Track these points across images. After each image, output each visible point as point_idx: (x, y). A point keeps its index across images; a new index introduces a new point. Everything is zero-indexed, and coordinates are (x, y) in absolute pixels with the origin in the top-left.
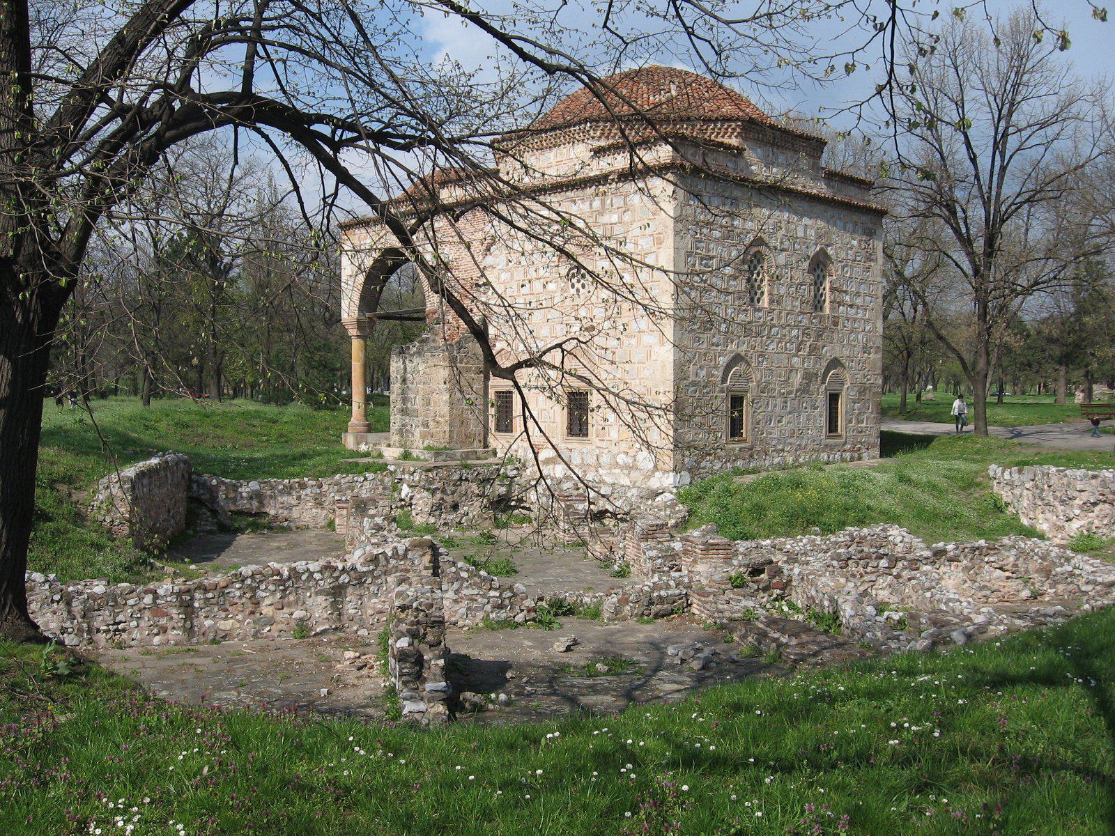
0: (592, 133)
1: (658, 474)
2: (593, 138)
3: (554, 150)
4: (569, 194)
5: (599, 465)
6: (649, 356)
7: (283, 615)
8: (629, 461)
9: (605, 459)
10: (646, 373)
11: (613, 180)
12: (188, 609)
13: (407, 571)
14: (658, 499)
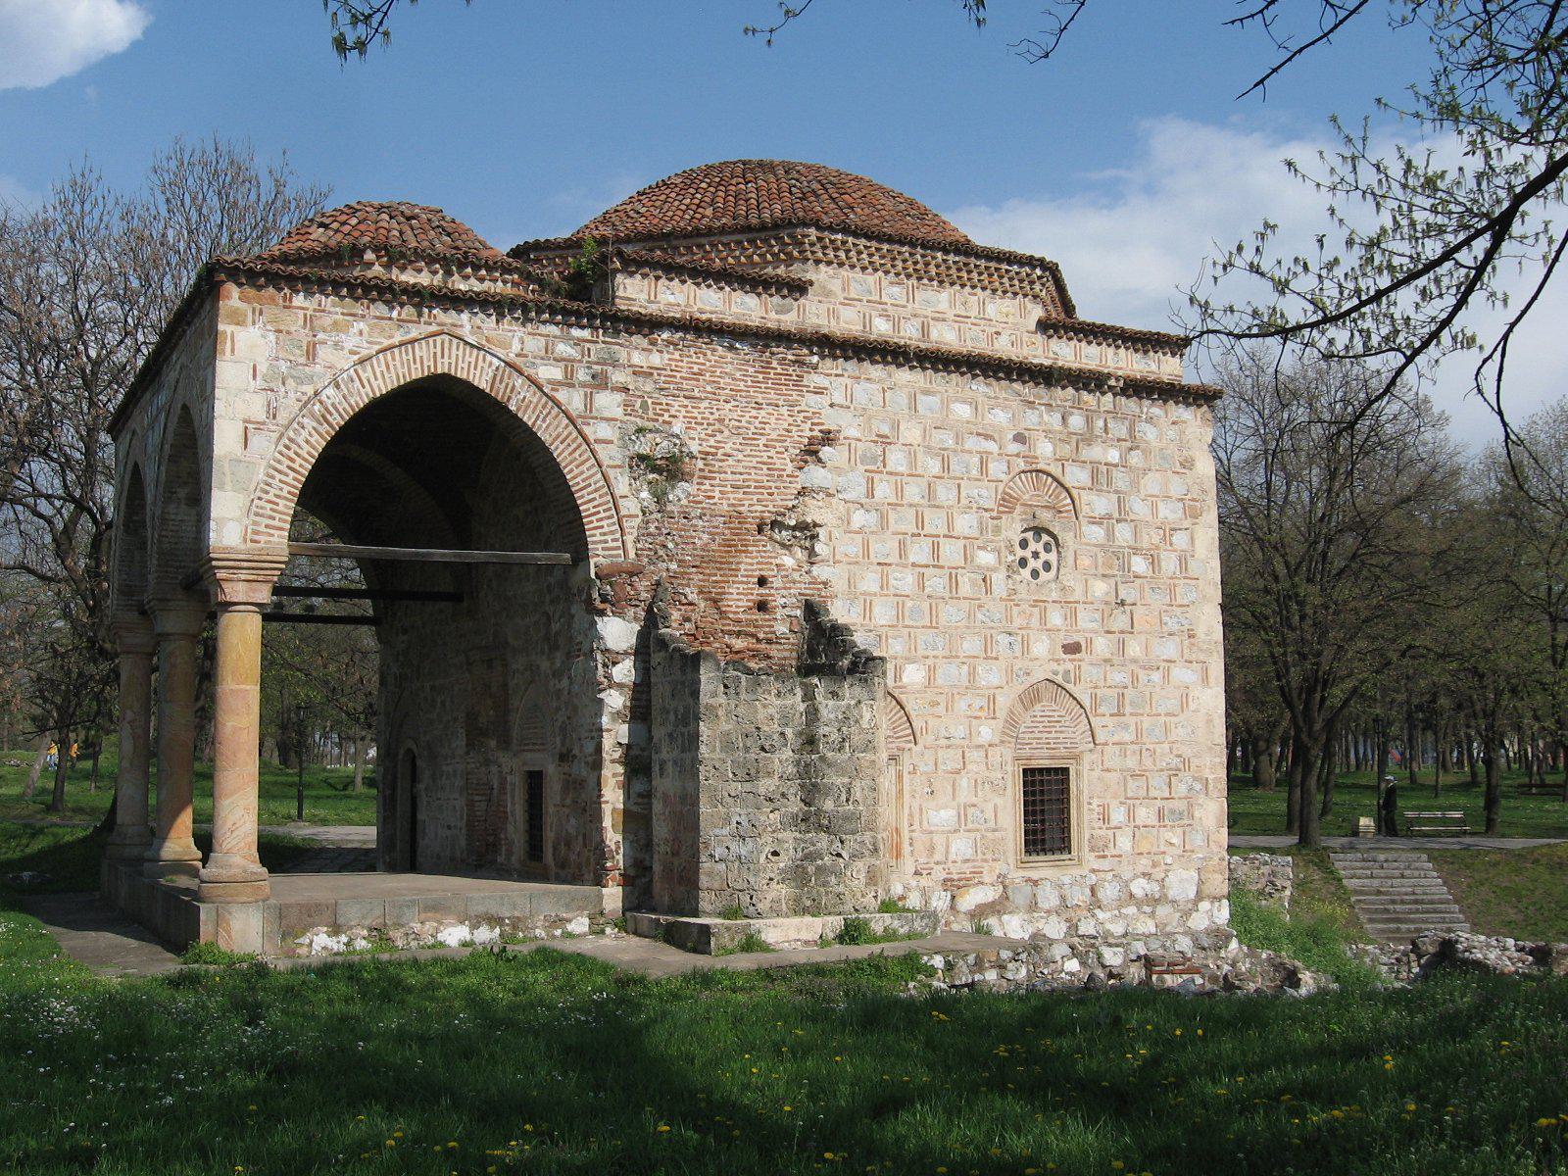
0: (1037, 287)
1: (1204, 905)
2: (1035, 297)
4: (1017, 386)
5: (1095, 903)
6: (1184, 701)
9: (1109, 892)
11: (1111, 388)
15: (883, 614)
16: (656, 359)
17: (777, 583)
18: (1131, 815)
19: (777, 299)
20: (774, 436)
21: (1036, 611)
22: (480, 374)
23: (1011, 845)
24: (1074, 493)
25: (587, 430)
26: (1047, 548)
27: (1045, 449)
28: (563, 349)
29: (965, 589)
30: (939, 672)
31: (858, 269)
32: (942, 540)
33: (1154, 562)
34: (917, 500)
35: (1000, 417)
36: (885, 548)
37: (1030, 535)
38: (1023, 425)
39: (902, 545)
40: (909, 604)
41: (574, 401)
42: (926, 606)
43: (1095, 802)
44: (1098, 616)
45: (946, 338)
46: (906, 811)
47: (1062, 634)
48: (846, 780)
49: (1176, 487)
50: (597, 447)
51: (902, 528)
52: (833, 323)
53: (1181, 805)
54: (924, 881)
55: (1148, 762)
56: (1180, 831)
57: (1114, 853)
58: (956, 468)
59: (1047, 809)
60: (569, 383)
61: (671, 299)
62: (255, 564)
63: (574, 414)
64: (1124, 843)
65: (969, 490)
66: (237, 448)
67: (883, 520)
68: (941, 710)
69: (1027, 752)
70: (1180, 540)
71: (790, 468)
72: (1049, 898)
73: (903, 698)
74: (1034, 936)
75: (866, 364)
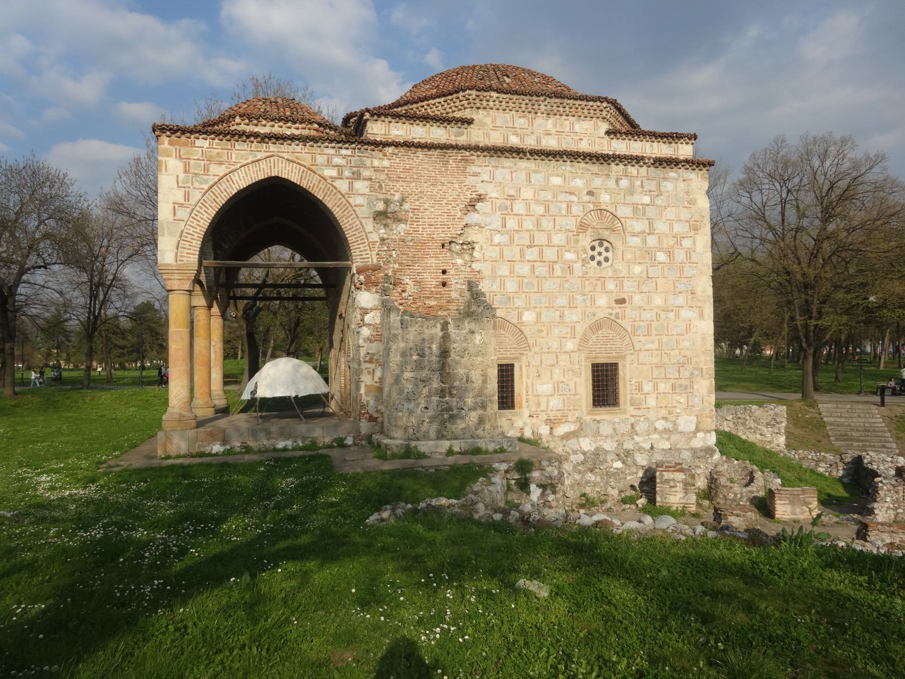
0: (604, 113)
1: (700, 435)
6: (688, 329)
8: (670, 425)
9: (641, 427)
10: (686, 344)
15: (511, 286)
16: (386, 163)
17: (452, 272)
18: (655, 387)
19: (455, 129)
20: (451, 198)
21: (599, 283)
22: (293, 175)
23: (584, 402)
24: (623, 220)
25: (351, 200)
26: (607, 250)
27: (605, 198)
28: (337, 160)
29: (558, 270)
30: (543, 316)
31: (501, 111)
32: (544, 248)
33: (670, 254)
34: (531, 227)
35: (579, 183)
36: (512, 252)
37: (596, 243)
38: (592, 186)
39: (522, 251)
40: (526, 281)
41: (343, 186)
42: (535, 281)
43: (634, 381)
44: (636, 284)
45: (551, 144)
46: (524, 385)
47: (614, 294)
48: (466, 371)
49: (685, 214)
50: (355, 208)
51: (522, 242)
52: (487, 140)
53: (683, 382)
54: (534, 420)
55: (666, 360)
56: (685, 396)
57: (645, 406)
58: (553, 210)
59: (605, 385)
60: (340, 177)
61: (398, 133)
62: (181, 270)
63: (343, 192)
64: (651, 402)
65: (562, 222)
66: (171, 217)
67: (512, 240)
68: (544, 334)
69: (594, 355)
70: (687, 243)
71: (459, 214)
72: (606, 429)
73: (523, 328)
74: (597, 449)
75: (503, 160)
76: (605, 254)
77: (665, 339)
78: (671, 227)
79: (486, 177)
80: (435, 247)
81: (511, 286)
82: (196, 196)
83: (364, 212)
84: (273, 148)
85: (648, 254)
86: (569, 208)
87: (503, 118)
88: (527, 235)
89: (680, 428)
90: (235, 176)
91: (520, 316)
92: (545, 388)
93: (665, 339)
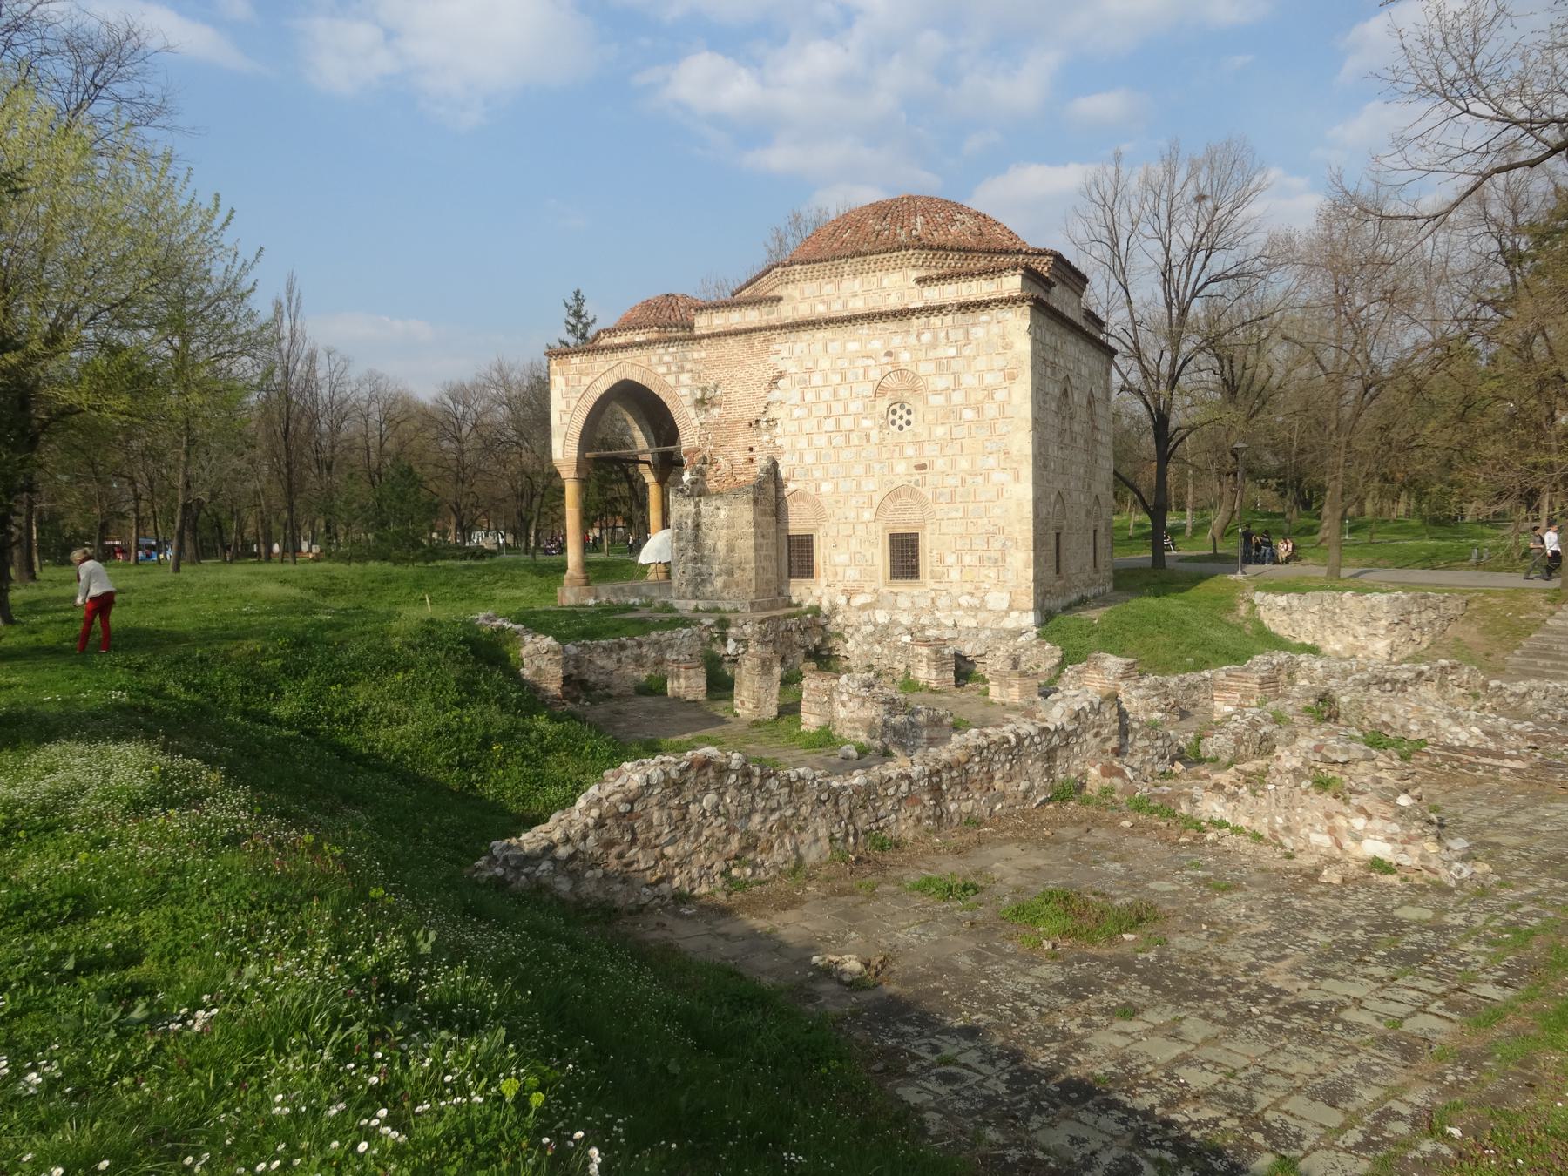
1: (1014, 614)
3: (860, 278)
6: (1000, 494)
7: (1010, 788)
8: (976, 602)
9: (943, 602)
10: (998, 511)
12: (936, 791)
13: (1101, 726)
14: (1022, 639)
15: (809, 459)
16: (703, 354)
18: (960, 559)
23: (880, 573)
26: (909, 412)
28: (667, 358)
33: (979, 411)
35: (877, 345)
37: (897, 407)
39: (819, 424)
41: (671, 380)
45: (858, 306)
49: (999, 362)
53: (993, 554)
54: (832, 590)
55: (972, 529)
58: (850, 377)
59: (905, 556)
60: (669, 373)
64: (955, 575)
65: (858, 388)
67: (810, 411)
70: (1000, 396)
72: (904, 602)
76: (906, 417)
77: (971, 506)
78: (981, 379)
79: (785, 354)
80: (743, 425)
81: (809, 459)
82: (574, 403)
83: (688, 401)
84: (621, 355)
85: (951, 414)
86: (866, 373)
87: (810, 288)
88: (824, 406)
89: (989, 606)
90: (598, 384)
91: (818, 488)
92: (841, 558)
93: (971, 506)
